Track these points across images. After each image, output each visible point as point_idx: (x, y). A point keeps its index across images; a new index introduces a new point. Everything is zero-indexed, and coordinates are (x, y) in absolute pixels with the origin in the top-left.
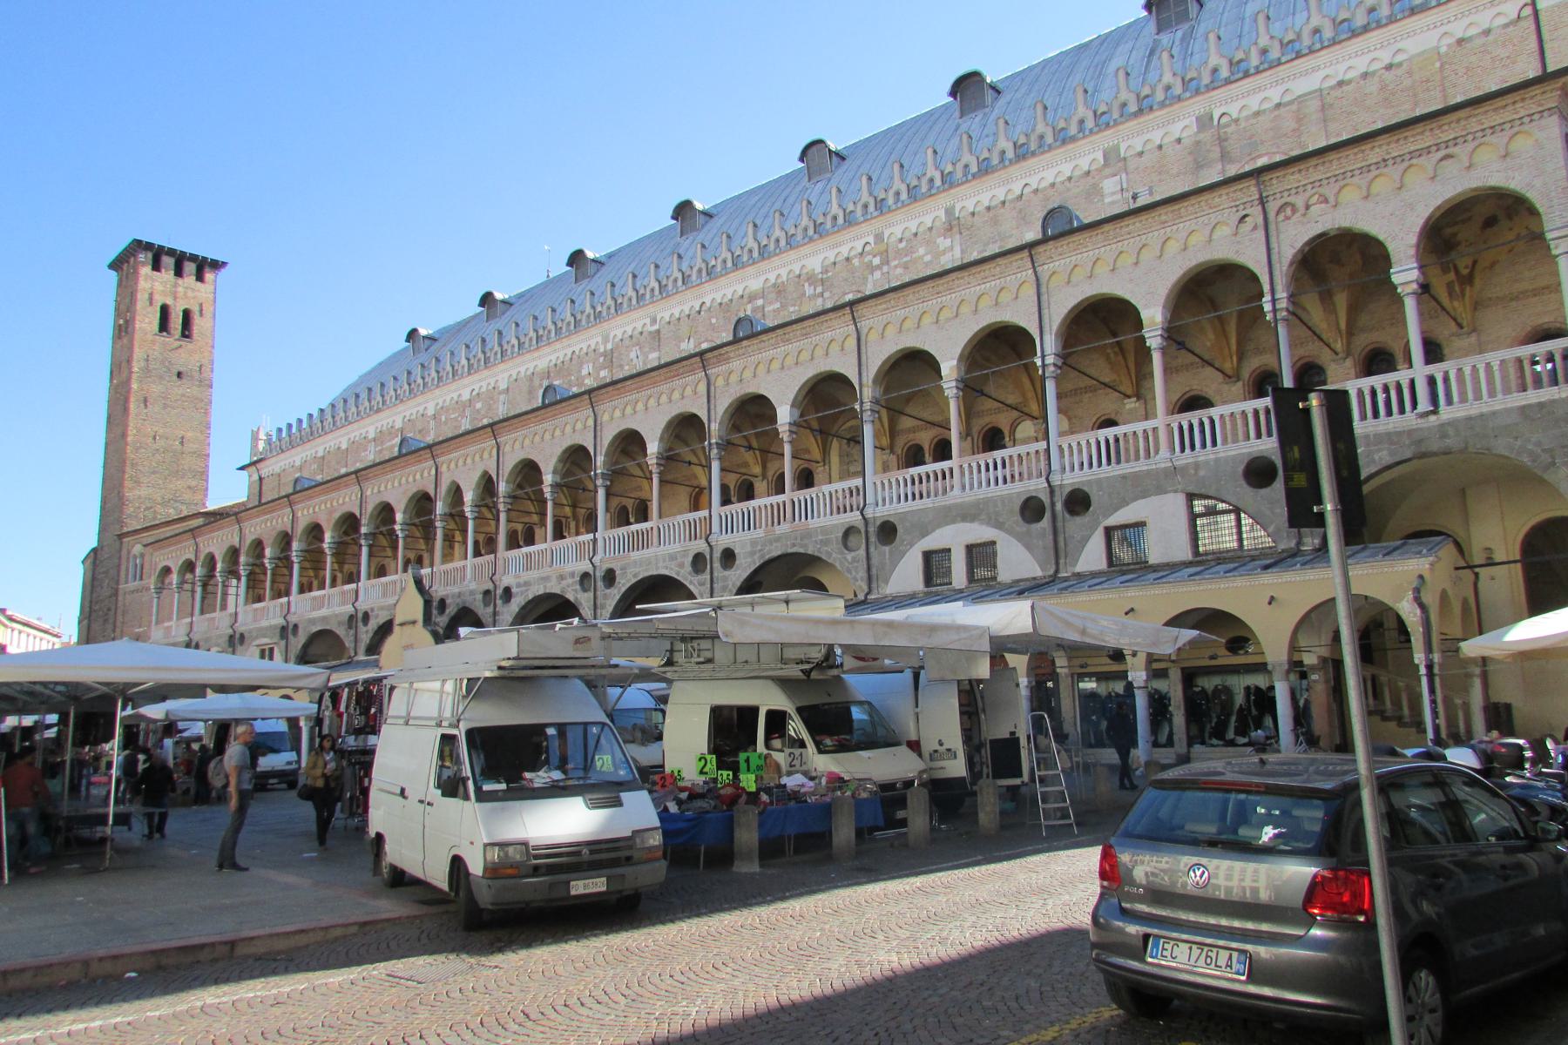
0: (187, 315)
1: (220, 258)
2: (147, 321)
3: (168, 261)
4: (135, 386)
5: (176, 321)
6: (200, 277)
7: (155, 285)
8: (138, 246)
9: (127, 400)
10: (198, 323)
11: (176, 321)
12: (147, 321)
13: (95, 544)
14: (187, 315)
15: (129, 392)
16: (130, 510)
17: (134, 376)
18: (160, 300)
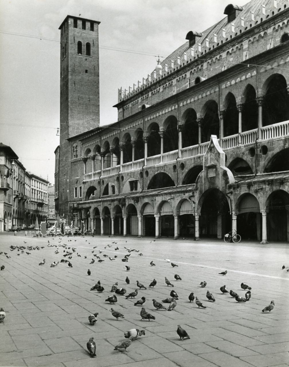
0: (88, 45)
1: (99, 21)
2: (73, 49)
3: (80, 23)
4: (70, 77)
5: (84, 48)
6: (92, 29)
7: (76, 33)
8: (69, 17)
9: (67, 84)
10: (92, 49)
11: (84, 48)
12: (73, 49)
13: (59, 144)
14: (88, 45)
15: (68, 79)
16: (70, 129)
17: (70, 73)
18: (77, 40)
